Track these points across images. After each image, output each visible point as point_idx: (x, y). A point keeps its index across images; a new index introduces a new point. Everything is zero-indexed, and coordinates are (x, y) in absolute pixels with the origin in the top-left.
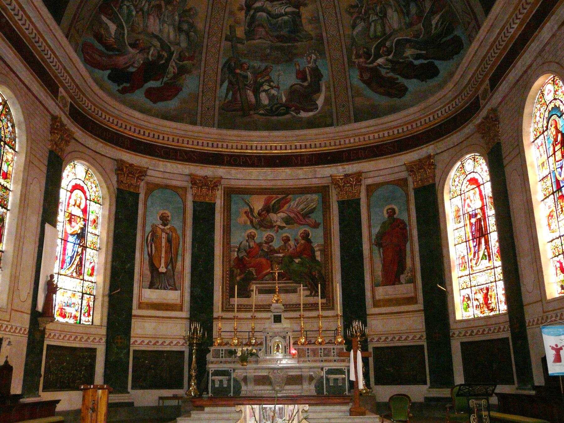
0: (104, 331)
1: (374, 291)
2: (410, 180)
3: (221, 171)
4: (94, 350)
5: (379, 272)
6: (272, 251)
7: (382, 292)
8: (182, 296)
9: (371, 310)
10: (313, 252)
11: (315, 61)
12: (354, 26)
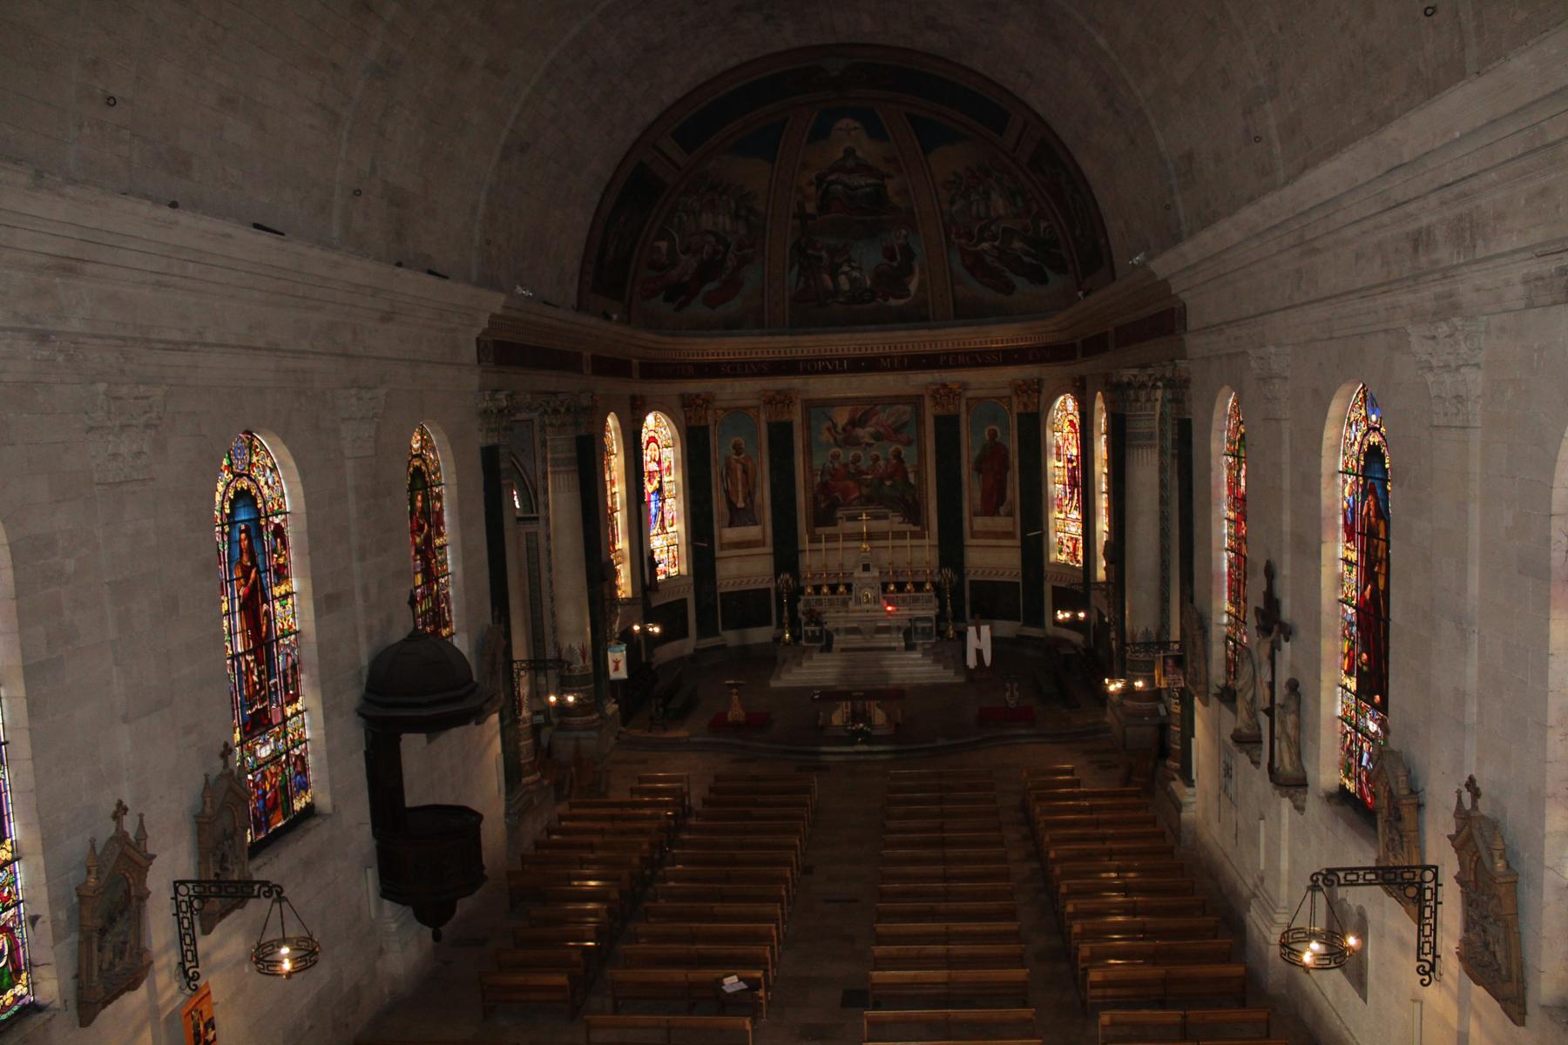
0: (691, 580)
1: (974, 522)
2: (1015, 399)
3: (796, 382)
4: (684, 601)
5: (978, 501)
6: (862, 473)
7: (981, 523)
8: (764, 531)
9: (969, 541)
10: (906, 473)
11: (906, 237)
12: (952, 203)
